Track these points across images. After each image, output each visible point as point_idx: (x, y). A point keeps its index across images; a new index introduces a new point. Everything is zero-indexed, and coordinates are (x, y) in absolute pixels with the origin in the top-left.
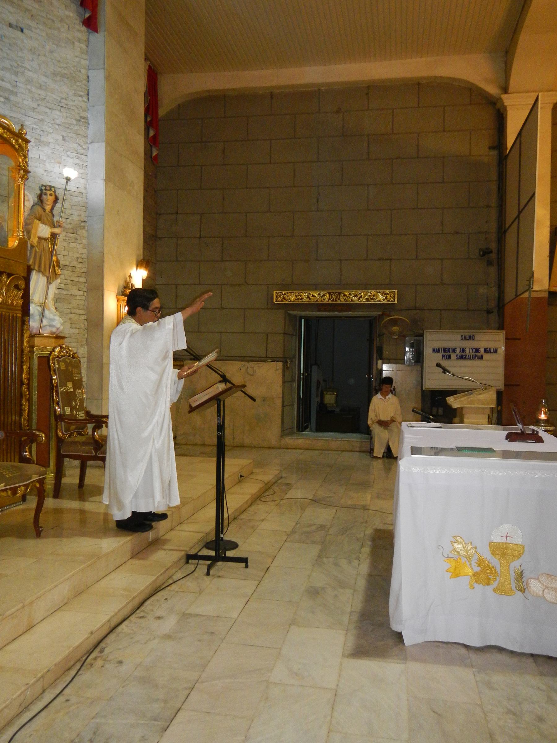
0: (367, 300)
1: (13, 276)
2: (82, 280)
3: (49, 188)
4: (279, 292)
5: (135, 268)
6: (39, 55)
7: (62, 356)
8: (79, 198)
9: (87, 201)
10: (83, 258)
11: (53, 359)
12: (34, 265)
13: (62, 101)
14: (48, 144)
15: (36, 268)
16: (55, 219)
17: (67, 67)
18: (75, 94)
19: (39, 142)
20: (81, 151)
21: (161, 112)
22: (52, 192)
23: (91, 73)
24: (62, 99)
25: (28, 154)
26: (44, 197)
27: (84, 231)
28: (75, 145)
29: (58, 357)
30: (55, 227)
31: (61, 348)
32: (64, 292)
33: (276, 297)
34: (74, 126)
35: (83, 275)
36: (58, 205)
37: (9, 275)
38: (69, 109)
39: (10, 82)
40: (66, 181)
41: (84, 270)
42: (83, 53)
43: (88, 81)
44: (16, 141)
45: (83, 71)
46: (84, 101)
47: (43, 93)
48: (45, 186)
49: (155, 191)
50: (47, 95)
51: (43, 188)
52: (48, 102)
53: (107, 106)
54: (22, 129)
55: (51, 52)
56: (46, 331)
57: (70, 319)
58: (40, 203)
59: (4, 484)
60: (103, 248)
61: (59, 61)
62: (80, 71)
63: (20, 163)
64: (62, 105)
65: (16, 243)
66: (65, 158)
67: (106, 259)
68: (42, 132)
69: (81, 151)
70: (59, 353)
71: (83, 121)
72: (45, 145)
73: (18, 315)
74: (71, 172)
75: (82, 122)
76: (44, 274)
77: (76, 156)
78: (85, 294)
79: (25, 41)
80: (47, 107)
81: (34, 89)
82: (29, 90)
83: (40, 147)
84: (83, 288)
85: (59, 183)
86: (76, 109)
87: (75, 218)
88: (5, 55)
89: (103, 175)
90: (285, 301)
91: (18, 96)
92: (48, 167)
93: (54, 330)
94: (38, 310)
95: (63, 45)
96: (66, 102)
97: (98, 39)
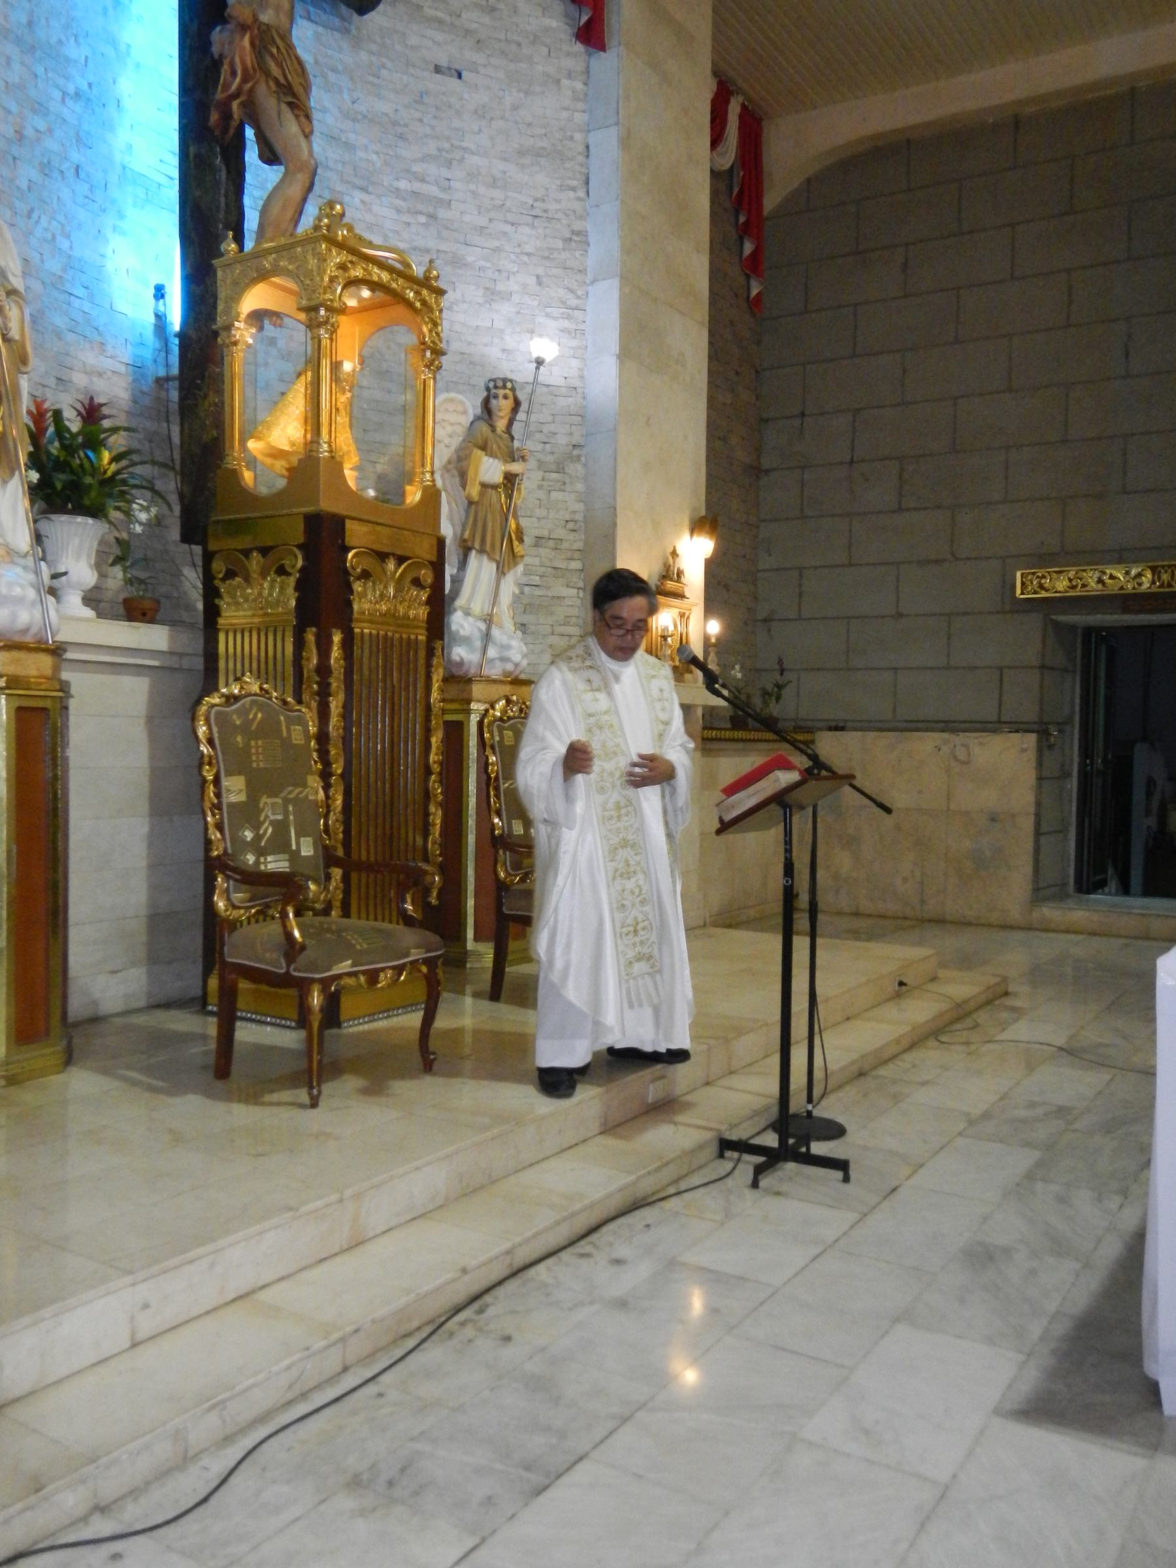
1: (410, 561)
2: (575, 565)
3: (500, 384)
4: (1029, 574)
5: (687, 535)
6: (492, 119)
7: (509, 718)
8: (570, 399)
9: (585, 403)
10: (576, 521)
11: (491, 724)
12: (473, 542)
13: (536, 204)
15: (477, 545)
16: (516, 444)
17: (545, 135)
18: (561, 186)
19: (493, 293)
20: (574, 302)
21: (771, 201)
22: (507, 391)
23: (593, 139)
24: (536, 200)
25: (441, 319)
26: (494, 402)
27: (579, 467)
28: (562, 292)
29: (501, 719)
30: (514, 461)
31: (509, 701)
32: (538, 592)
33: (1023, 584)
34: (560, 253)
35: (577, 555)
36: (521, 416)
37: (401, 560)
38: (549, 219)
39: (437, 183)
40: (535, 365)
41: (579, 545)
42: (579, 100)
43: (588, 156)
44: (417, 293)
45: (578, 136)
46: (579, 199)
47: (497, 194)
48: (494, 380)
49: (757, 372)
50: (506, 197)
51: (491, 385)
52: (509, 211)
53: (623, 202)
54: (429, 271)
55: (515, 108)
56: (495, 672)
57: (551, 646)
58: (486, 417)
59: (349, 962)
60: (614, 498)
61: (529, 125)
62: (572, 138)
63: (424, 337)
64: (535, 212)
65: (418, 497)
66: (540, 319)
67: (619, 521)
68: (497, 273)
69: (574, 302)
70: (504, 712)
71: (579, 239)
72: (503, 298)
73: (420, 637)
74: (545, 347)
75: (575, 241)
76: (491, 558)
77: (563, 313)
78: (581, 595)
79: (466, 96)
80: (506, 222)
81: (482, 190)
82: (473, 192)
83: (493, 303)
84: (576, 583)
85: (522, 373)
86: (564, 217)
87: (562, 440)
88: (428, 130)
89: (614, 346)
90: (1043, 592)
91: (452, 207)
92: (510, 341)
93: (509, 667)
94: (480, 630)
95: (538, 89)
97: (606, 63)
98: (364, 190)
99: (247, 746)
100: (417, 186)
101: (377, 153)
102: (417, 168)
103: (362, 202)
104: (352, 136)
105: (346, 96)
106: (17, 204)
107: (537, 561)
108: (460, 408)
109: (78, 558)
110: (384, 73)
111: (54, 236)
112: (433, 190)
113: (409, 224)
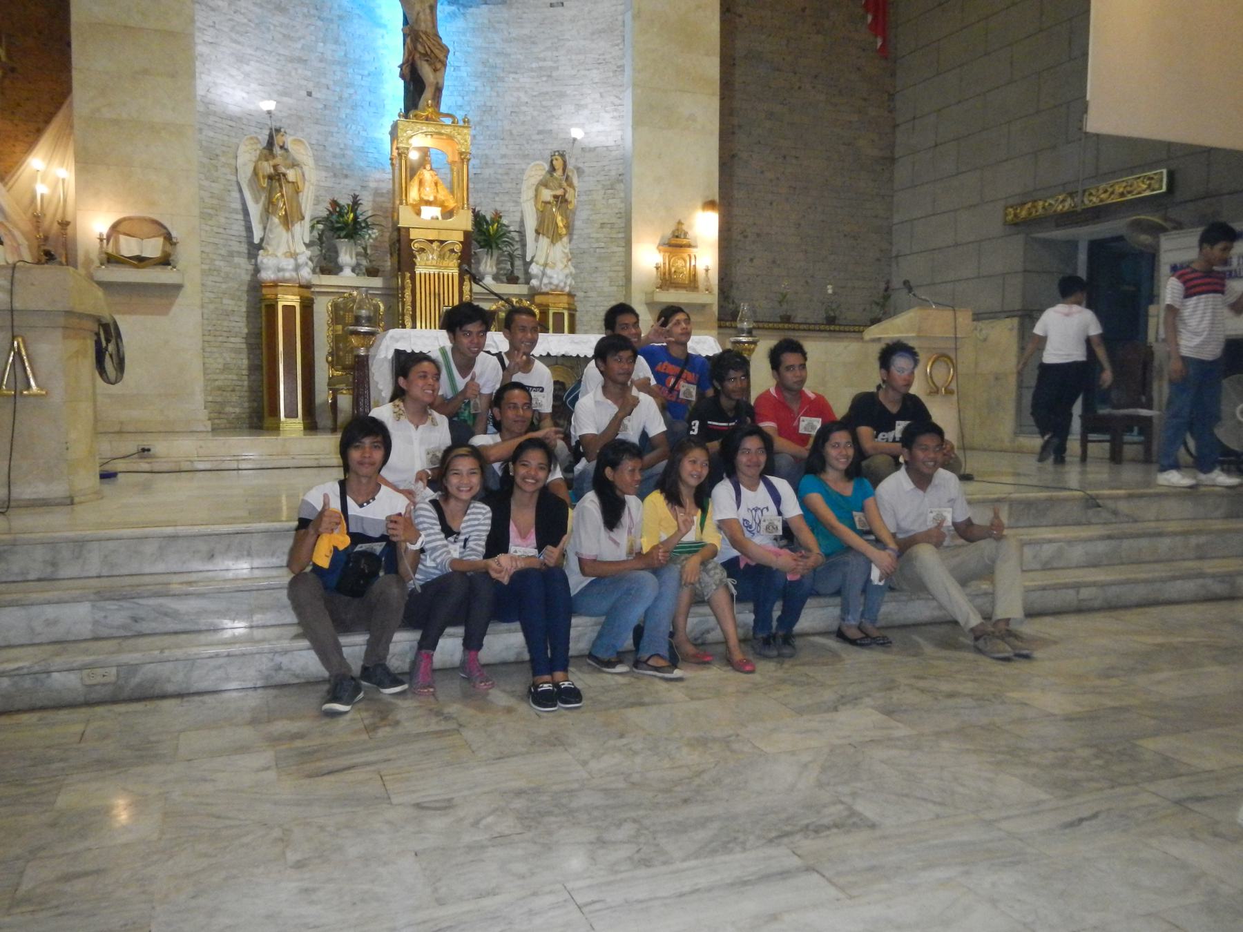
0: (1122, 195)
2: (621, 235)
14: (585, 106)
27: (622, 185)
28: (613, 99)
32: (603, 251)
35: (622, 230)
46: (620, 49)
47: (581, 57)
52: (587, 64)
55: (589, 12)
57: (609, 277)
61: (596, 19)
62: (617, 20)
69: (617, 101)
71: (621, 68)
76: (548, 237)
81: (574, 57)
87: (613, 173)
89: (630, 122)
93: (553, 287)
96: (604, 57)
98: (516, 73)
99: (344, 315)
100: (541, 64)
101: (521, 54)
102: (542, 55)
103: (514, 78)
104: (509, 50)
105: (506, 33)
106: (340, 124)
107: (602, 235)
108: (542, 168)
109: (346, 254)
110: (525, 16)
111: (359, 132)
112: (550, 64)
113: (537, 83)
